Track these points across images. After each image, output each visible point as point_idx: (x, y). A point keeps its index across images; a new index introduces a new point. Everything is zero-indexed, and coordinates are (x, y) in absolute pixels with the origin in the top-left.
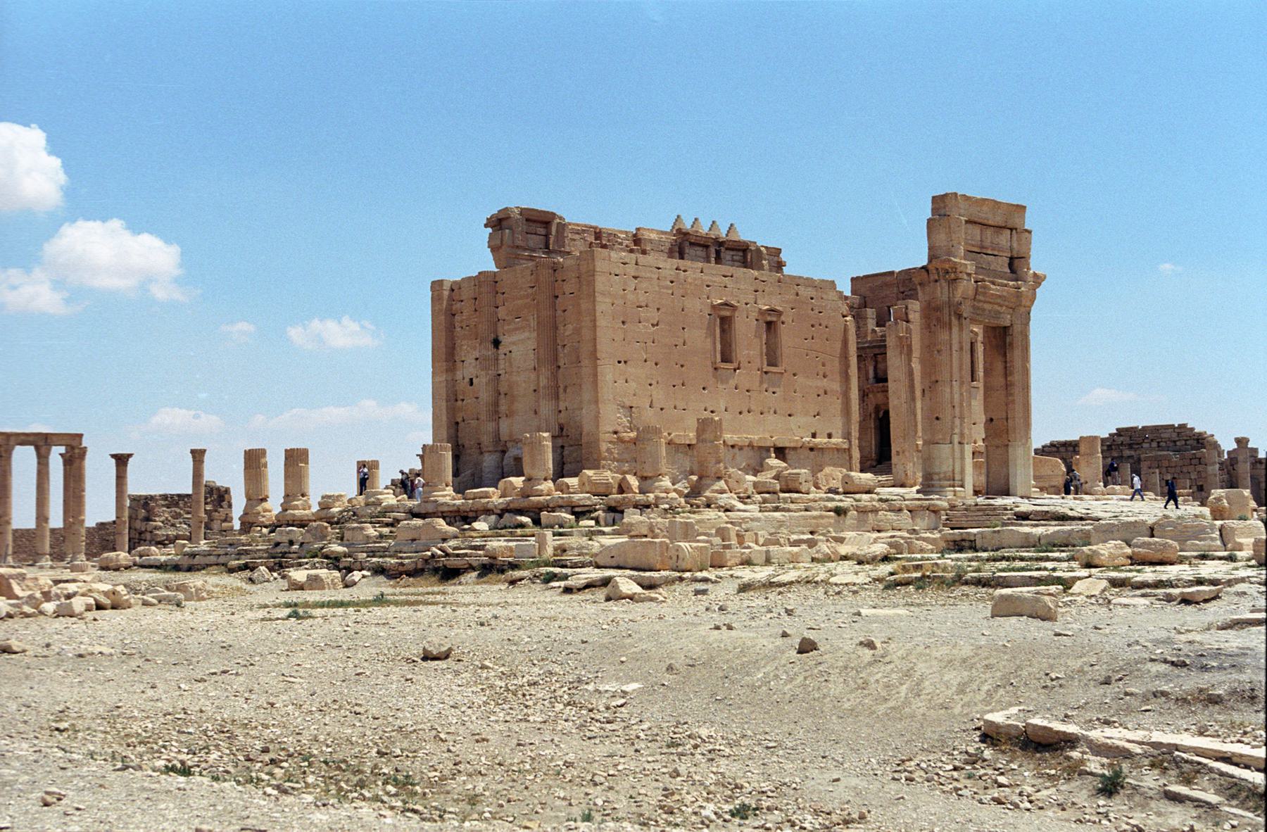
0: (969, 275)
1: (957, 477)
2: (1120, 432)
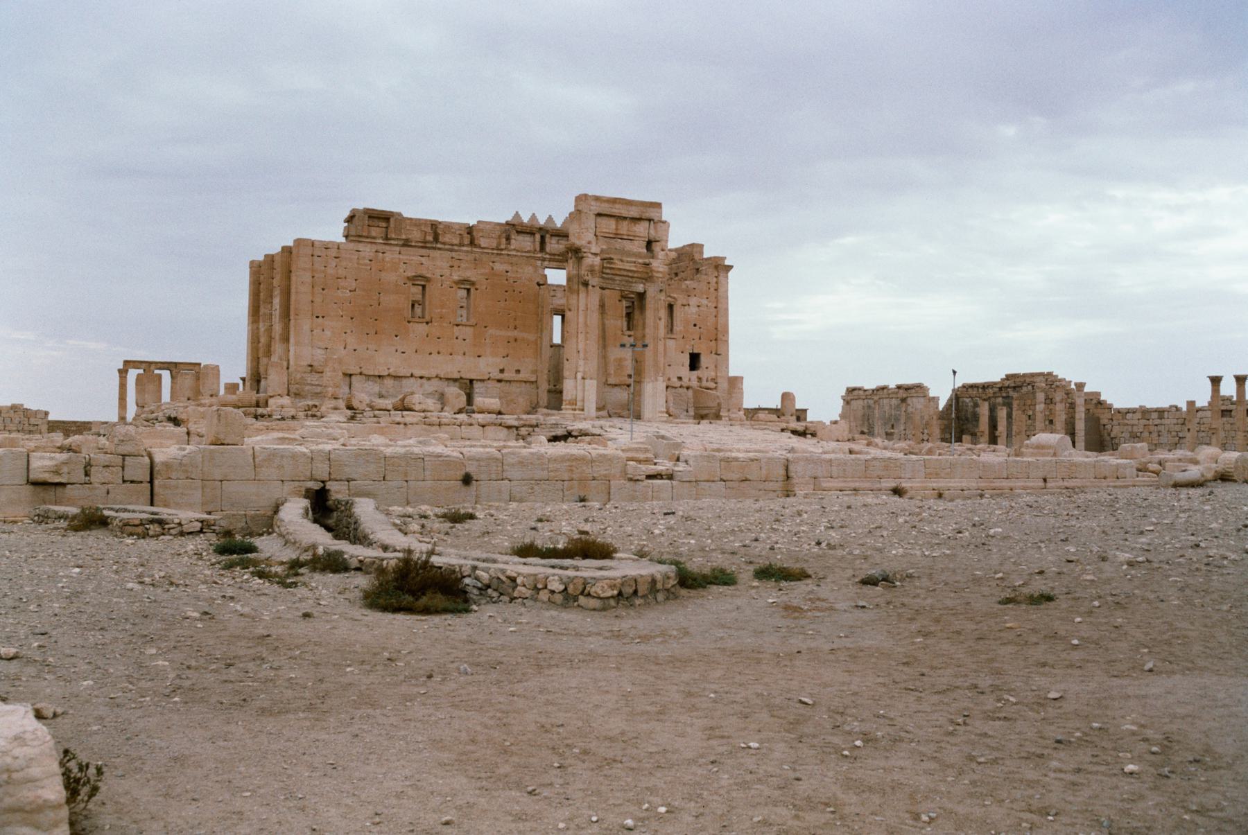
0: (596, 254)
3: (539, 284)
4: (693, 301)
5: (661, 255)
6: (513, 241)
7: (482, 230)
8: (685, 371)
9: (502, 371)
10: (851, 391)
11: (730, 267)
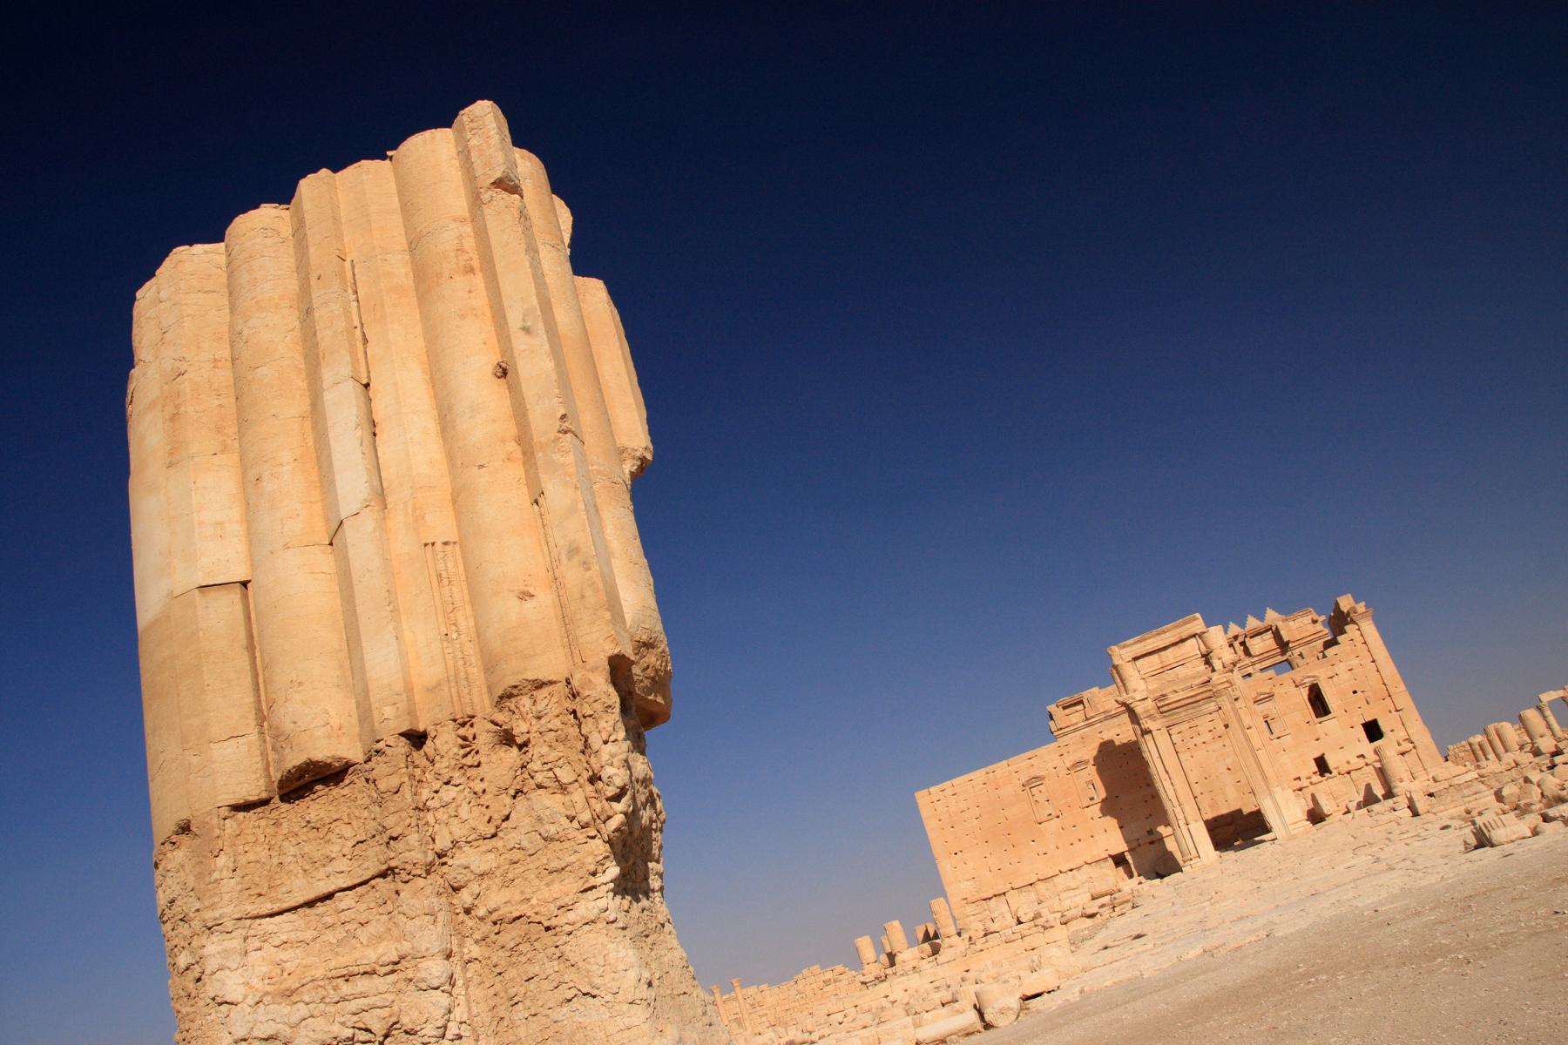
4: (1341, 668)
8: (1367, 747)
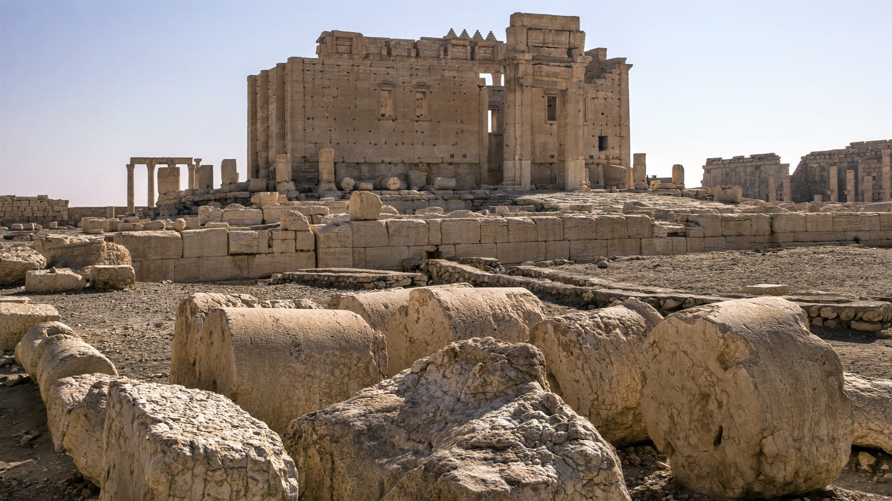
1: (517, 180)
2: (853, 145)
3: (480, 87)
4: (601, 94)
5: (579, 59)
6: (449, 53)
7: (425, 45)
8: (595, 152)
9: (452, 156)
10: (710, 162)
11: (631, 66)
